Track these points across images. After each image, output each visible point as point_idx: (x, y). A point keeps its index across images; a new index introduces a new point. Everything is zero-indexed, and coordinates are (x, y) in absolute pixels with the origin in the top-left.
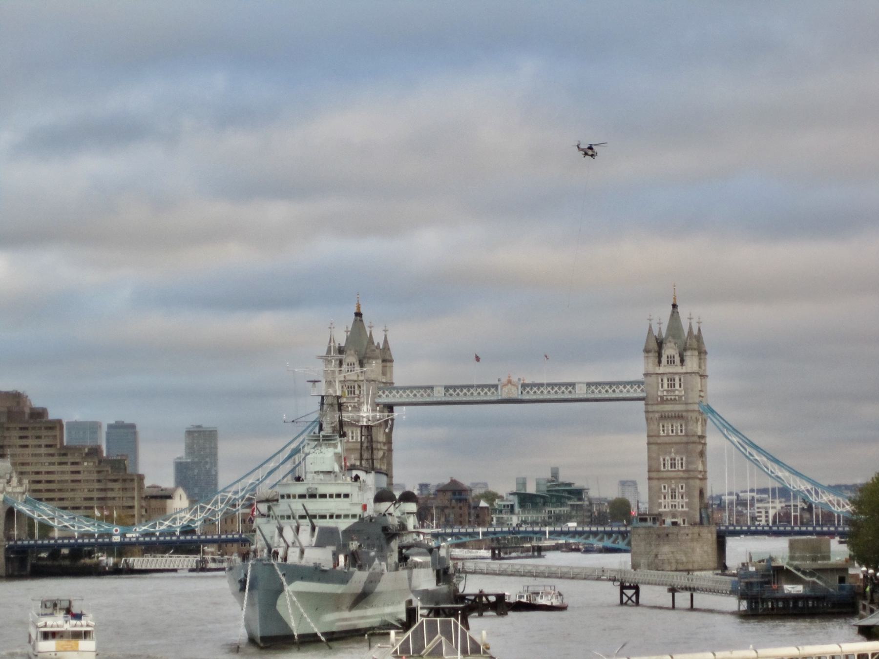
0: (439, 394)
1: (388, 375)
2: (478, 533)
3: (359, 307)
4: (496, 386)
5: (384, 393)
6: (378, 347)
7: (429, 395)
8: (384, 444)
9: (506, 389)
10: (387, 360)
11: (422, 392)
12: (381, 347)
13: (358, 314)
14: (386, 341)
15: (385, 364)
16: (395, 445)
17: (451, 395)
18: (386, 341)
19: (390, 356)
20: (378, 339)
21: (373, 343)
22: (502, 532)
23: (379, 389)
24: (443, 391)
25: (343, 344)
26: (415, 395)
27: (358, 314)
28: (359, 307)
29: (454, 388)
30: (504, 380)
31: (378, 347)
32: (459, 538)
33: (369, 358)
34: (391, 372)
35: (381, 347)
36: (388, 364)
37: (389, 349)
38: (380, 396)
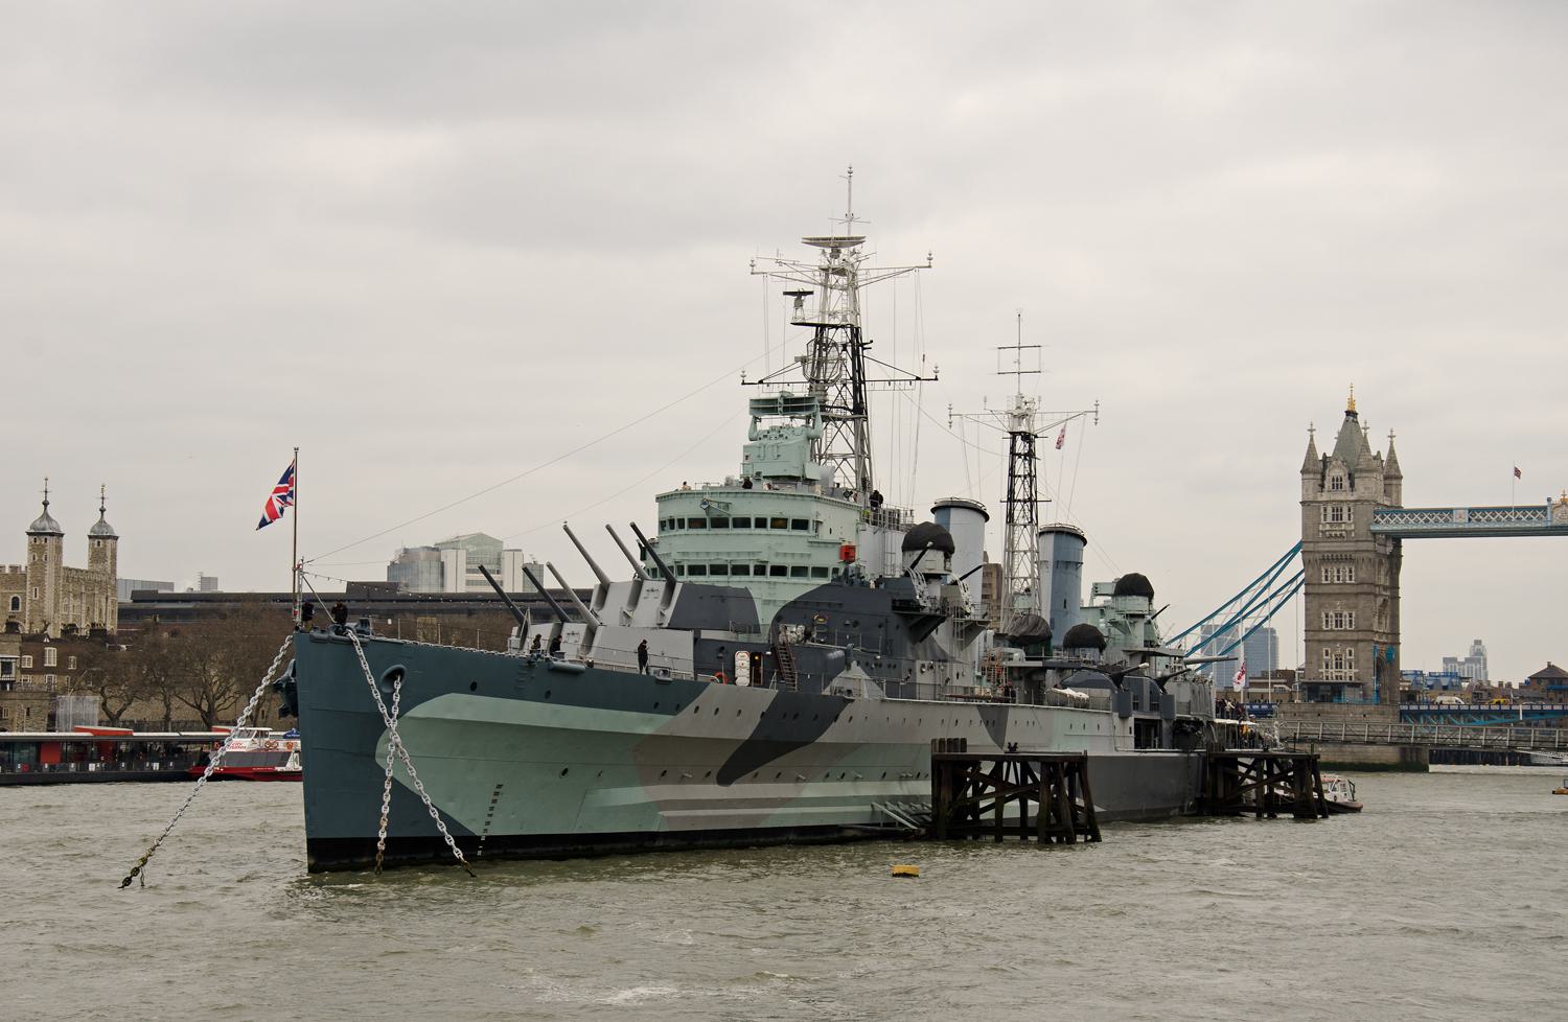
0: (1460, 522)
1: (1394, 496)
2: (1517, 712)
3: (1352, 402)
4: (1544, 508)
5: (1383, 518)
6: (1378, 457)
7: (1446, 521)
8: (1385, 588)
9: (1558, 512)
10: (1392, 477)
11: (1436, 516)
12: (1384, 457)
13: (1351, 414)
14: (1392, 451)
15: (1388, 482)
16: (1401, 593)
17: (1479, 520)
18: (1392, 451)
19: (1398, 470)
20: (1378, 445)
21: (1368, 450)
22: (1553, 711)
23: (1376, 513)
24: (1466, 515)
25: (1329, 454)
26: (1427, 521)
27: (1351, 414)
28: (1352, 402)
29: (1483, 510)
30: (1556, 500)
31: (1378, 457)
32: (1490, 719)
33: (1361, 471)
34: (1399, 493)
35: (1384, 457)
36: (1394, 482)
37: (1396, 462)
38: (1377, 522)
